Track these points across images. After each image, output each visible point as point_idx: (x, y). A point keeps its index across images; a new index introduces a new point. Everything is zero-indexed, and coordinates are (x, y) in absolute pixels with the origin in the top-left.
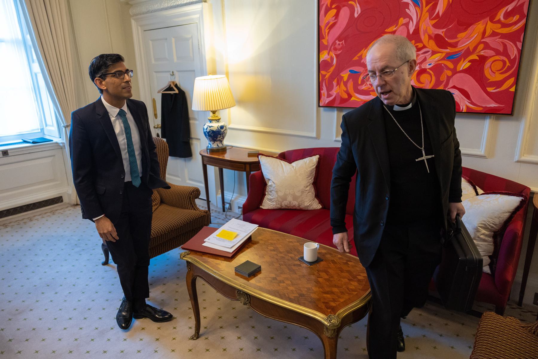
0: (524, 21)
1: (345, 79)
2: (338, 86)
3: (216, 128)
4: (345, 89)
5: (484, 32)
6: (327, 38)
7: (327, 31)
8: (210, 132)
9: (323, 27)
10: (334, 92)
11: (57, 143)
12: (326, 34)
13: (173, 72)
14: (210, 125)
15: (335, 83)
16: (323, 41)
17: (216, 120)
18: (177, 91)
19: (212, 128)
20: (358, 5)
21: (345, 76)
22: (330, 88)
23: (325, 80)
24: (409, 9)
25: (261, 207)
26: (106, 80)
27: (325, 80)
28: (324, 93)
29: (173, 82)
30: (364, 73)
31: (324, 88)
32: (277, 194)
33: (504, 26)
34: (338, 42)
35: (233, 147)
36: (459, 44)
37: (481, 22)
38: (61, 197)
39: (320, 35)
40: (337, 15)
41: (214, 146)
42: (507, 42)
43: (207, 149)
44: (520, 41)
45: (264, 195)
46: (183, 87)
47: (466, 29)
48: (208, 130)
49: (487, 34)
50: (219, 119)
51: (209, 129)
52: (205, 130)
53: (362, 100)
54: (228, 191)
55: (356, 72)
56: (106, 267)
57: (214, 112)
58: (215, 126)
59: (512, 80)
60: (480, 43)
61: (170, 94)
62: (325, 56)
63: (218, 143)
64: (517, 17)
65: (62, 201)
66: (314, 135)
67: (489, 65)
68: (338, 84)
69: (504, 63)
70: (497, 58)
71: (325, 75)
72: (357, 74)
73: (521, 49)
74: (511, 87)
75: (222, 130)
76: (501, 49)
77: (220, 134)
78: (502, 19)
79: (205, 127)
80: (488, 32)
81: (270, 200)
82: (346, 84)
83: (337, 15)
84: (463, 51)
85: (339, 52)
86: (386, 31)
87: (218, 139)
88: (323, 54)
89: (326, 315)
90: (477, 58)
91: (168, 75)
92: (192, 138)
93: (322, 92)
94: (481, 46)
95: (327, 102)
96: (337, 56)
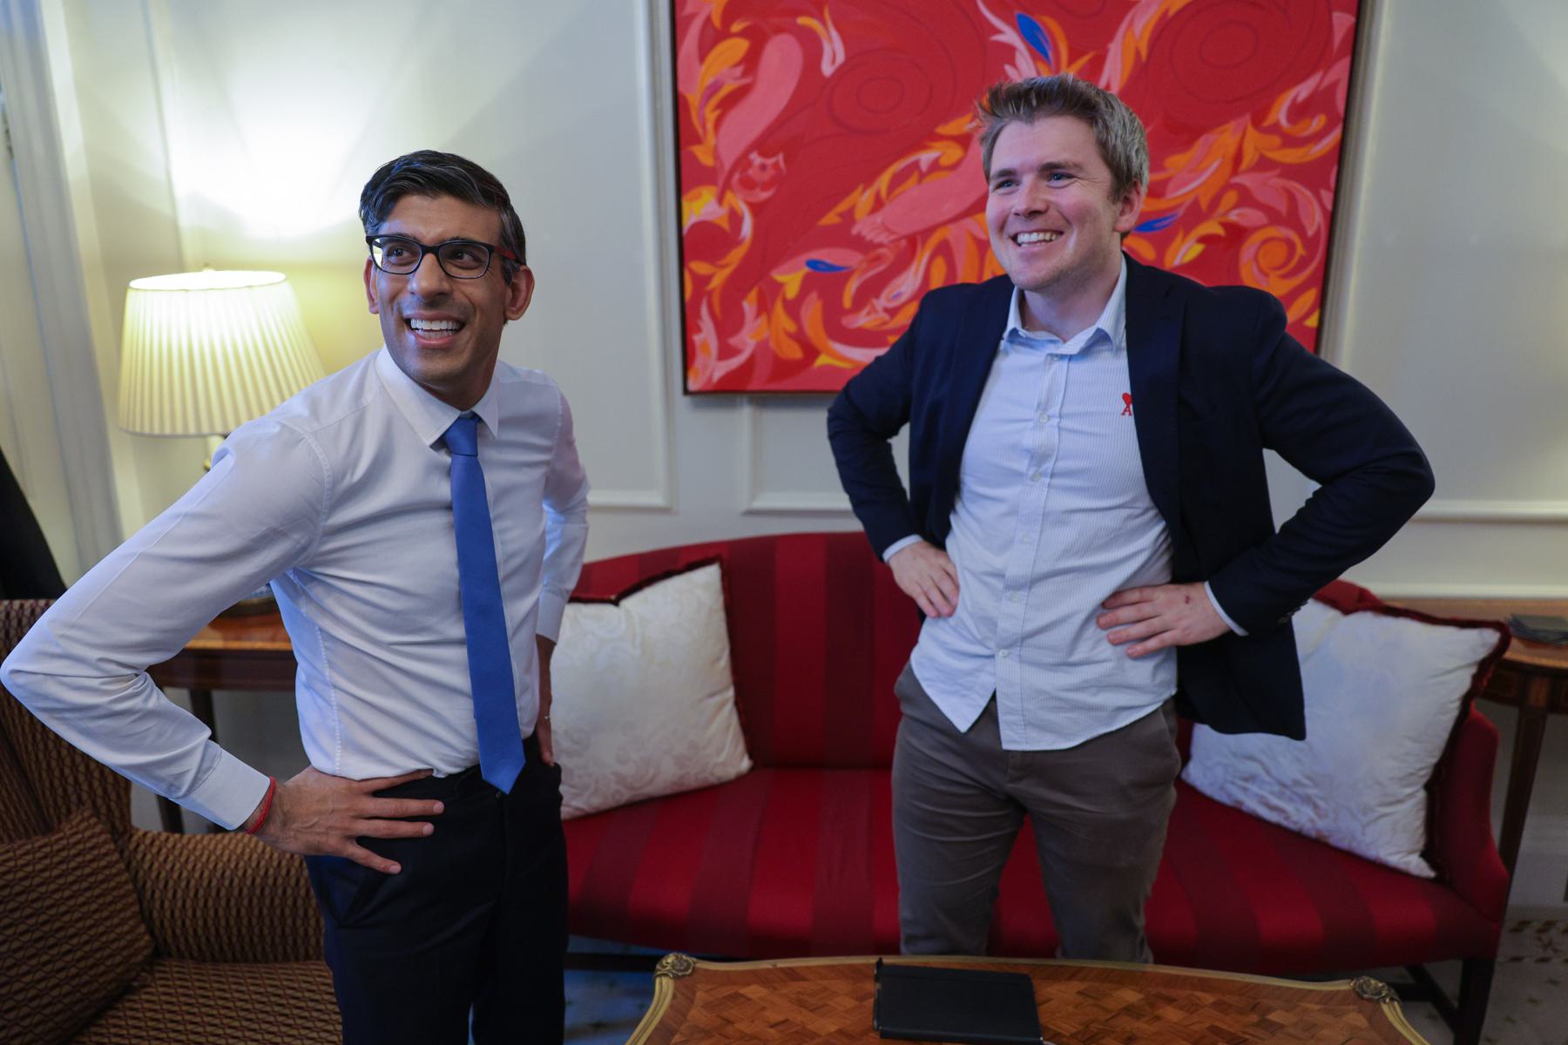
0: (1336, 134)
1: (792, 291)
2: (763, 318)
4: (791, 326)
5: (1238, 158)
6: (711, 140)
7: (711, 117)
9: (693, 98)
10: (746, 342)
12: (710, 126)
15: (749, 305)
16: (698, 150)
20: (834, 34)
21: (791, 280)
22: (728, 324)
23: (710, 294)
24: (1014, 65)
26: (1277, 287)
27: (710, 294)
28: (705, 344)
30: (866, 271)
31: (707, 324)
33: (1290, 141)
34: (756, 159)
36: (1171, 186)
37: (1231, 126)
39: (682, 127)
40: (751, 62)
42: (1295, 186)
44: (1328, 188)
47: (1187, 144)
49: (1245, 165)
55: (831, 268)
59: (1310, 296)
60: (1227, 187)
62: (703, 206)
64: (1318, 122)
66: (656, 499)
67: (1252, 251)
68: (764, 308)
69: (1291, 246)
70: (1273, 231)
71: (708, 279)
72: (839, 276)
73: (1329, 207)
74: (1308, 315)
76: (1282, 206)
78: (1284, 122)
80: (1249, 157)
82: (793, 308)
83: (751, 62)
84: (1181, 211)
85: (764, 195)
86: (941, 130)
88: (699, 196)
90: (1220, 231)
93: (697, 339)
94: (1231, 197)
95: (717, 376)
96: (756, 209)
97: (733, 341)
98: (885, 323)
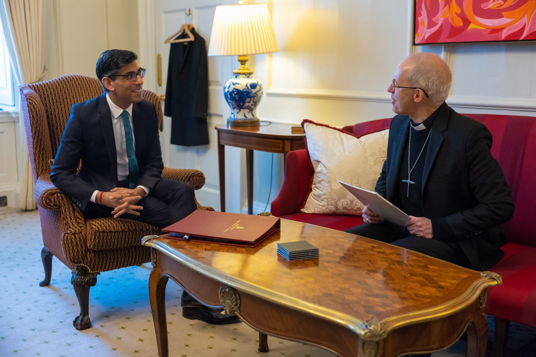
3: (244, 87)
4: (459, 11)
8: (233, 92)
10: (440, 19)
11: (8, 113)
13: (190, 10)
14: (235, 81)
17: (245, 74)
18: (192, 38)
19: (237, 87)
25: (302, 210)
28: (423, 21)
29: (189, 26)
31: (424, 12)
32: (330, 186)
35: (271, 123)
38: (5, 198)
41: (240, 116)
43: (228, 122)
45: (309, 190)
46: (202, 34)
48: (231, 90)
50: (250, 74)
51: (232, 87)
52: (226, 90)
53: (487, 28)
54: (260, 201)
56: (45, 289)
57: (243, 62)
58: (243, 83)
61: (182, 43)
63: (246, 111)
65: (6, 204)
75: (254, 91)
77: (250, 97)
79: (227, 85)
81: (318, 197)
87: (247, 104)
89: (362, 319)
91: (182, 15)
92: (210, 115)
95: (427, 36)
97: (433, 19)
98: (502, 5)
